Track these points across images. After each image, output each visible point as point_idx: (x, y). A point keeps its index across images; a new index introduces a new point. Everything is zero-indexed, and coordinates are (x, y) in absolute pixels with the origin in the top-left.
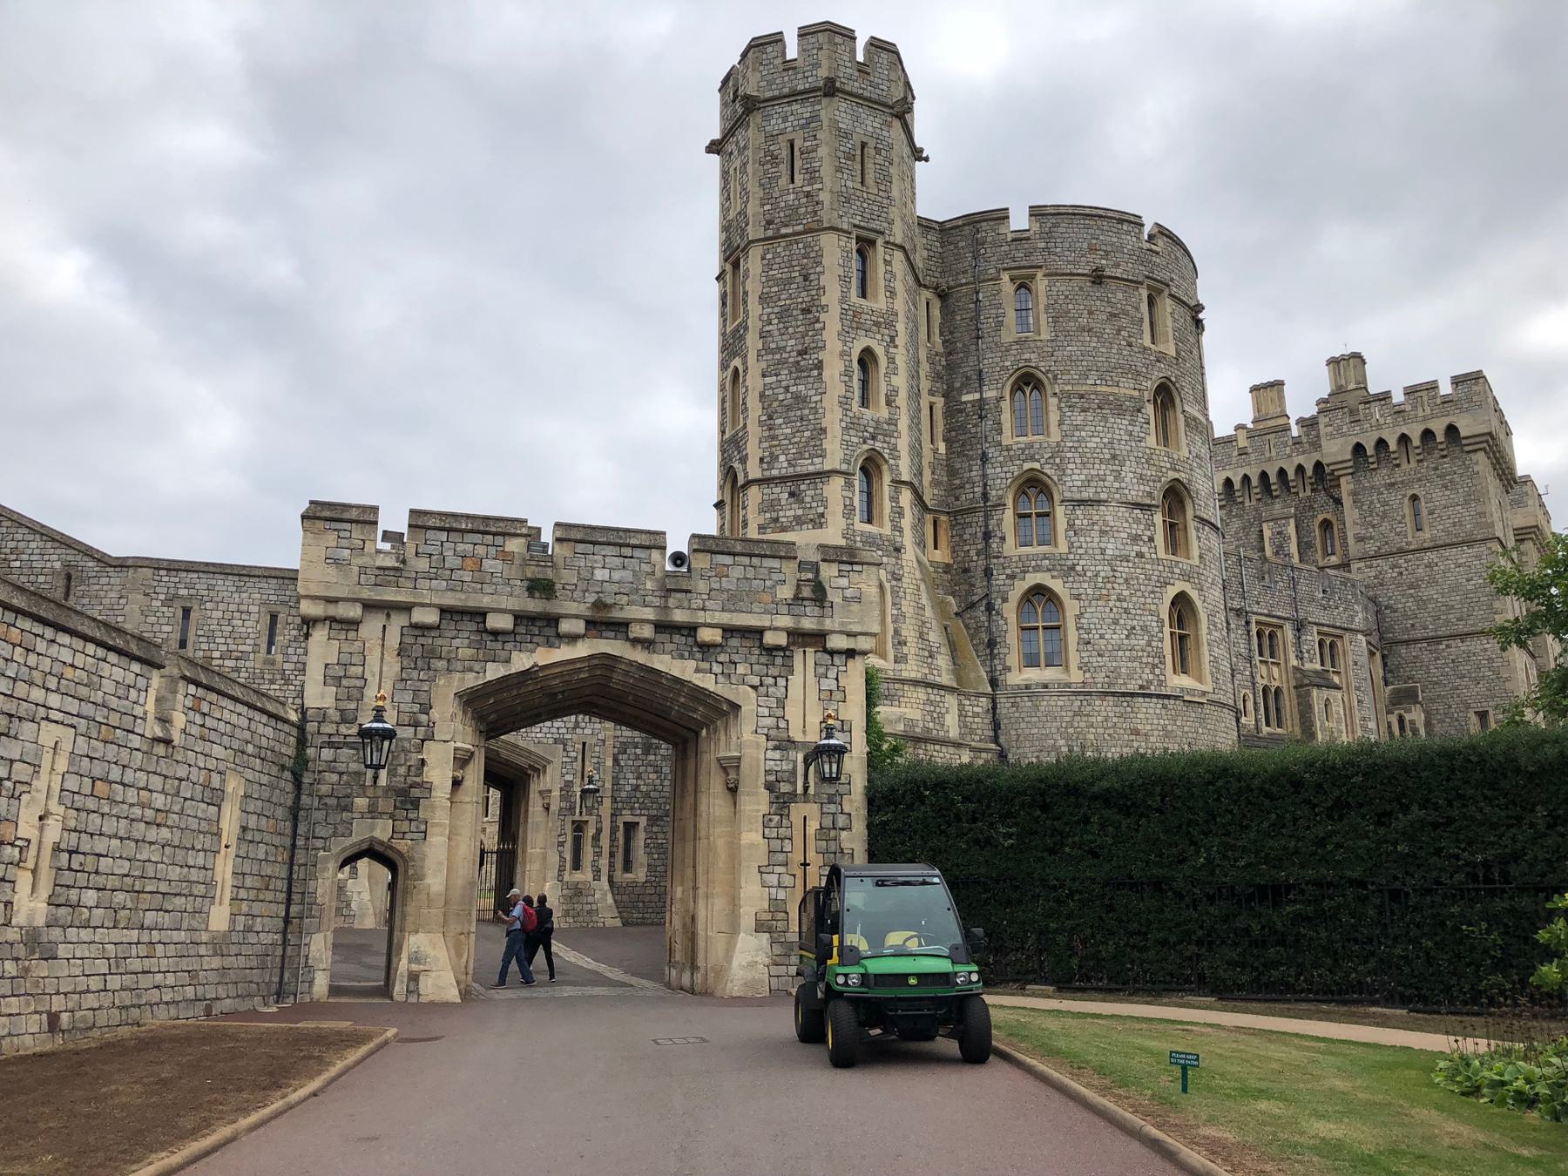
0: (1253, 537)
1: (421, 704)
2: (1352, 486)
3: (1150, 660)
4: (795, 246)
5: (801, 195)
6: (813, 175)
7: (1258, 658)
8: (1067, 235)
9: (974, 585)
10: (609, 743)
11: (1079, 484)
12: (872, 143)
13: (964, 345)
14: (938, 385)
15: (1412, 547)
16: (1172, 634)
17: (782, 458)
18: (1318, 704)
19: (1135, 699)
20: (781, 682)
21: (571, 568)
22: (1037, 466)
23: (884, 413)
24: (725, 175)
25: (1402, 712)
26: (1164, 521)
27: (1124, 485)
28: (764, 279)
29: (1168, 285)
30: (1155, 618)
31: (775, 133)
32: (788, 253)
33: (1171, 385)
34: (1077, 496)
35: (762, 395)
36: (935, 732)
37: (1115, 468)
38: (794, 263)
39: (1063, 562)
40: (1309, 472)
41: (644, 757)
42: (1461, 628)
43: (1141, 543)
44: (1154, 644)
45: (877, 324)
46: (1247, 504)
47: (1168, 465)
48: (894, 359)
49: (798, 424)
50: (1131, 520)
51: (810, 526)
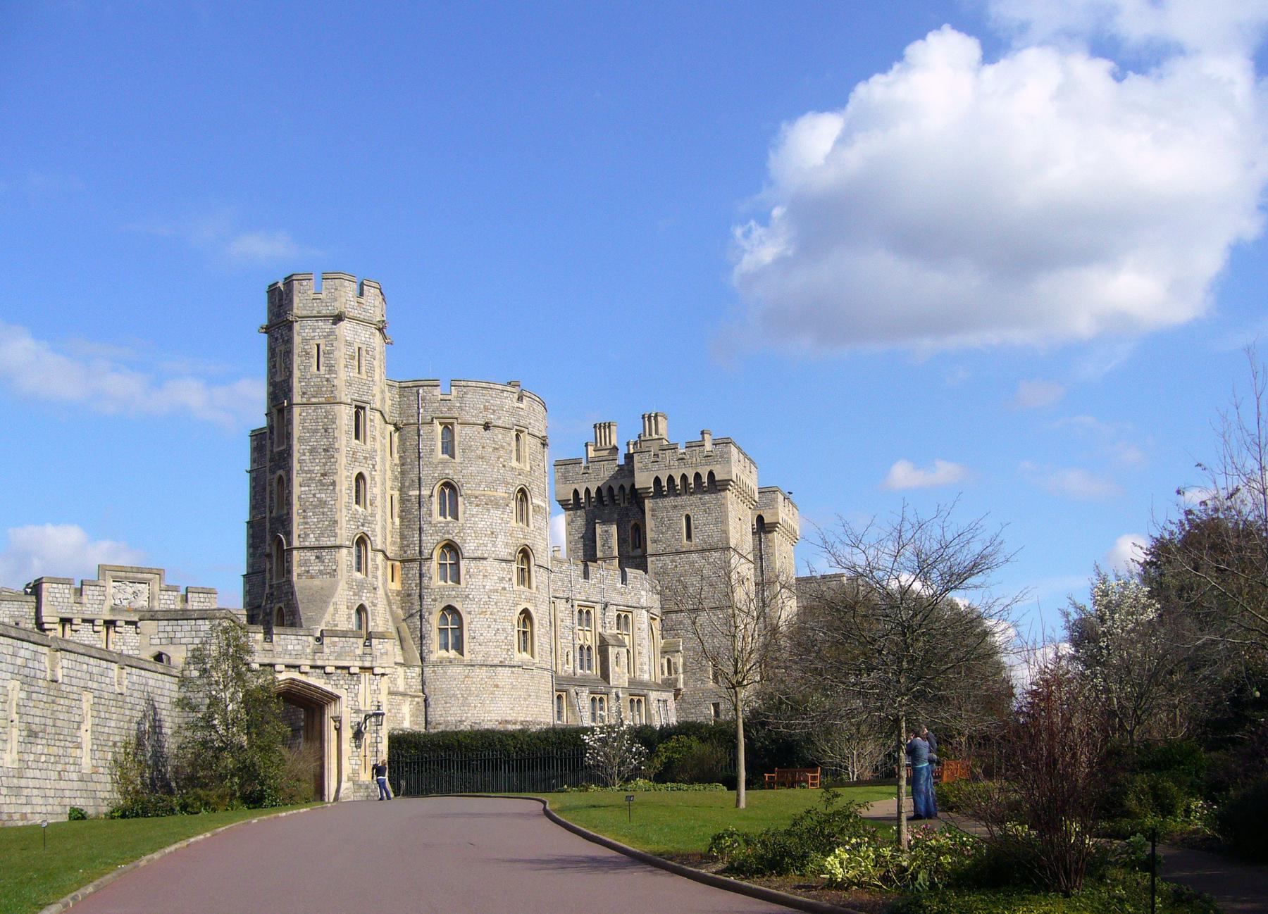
4: (320, 410)
5: (323, 380)
6: (331, 369)
8: (471, 400)
12: (364, 347)
13: (411, 461)
14: (396, 484)
15: (684, 550)
16: (518, 631)
17: (312, 536)
18: (612, 657)
20: (356, 687)
21: (279, 645)
22: (450, 537)
25: (670, 657)
26: (518, 568)
27: (497, 549)
28: (301, 428)
30: (510, 624)
31: (308, 338)
34: (472, 556)
37: (493, 539)
38: (320, 420)
39: (463, 593)
40: (627, 491)
43: (504, 582)
44: (508, 638)
45: (365, 458)
47: (522, 536)
48: (374, 478)
49: (321, 516)
50: (500, 569)
51: (328, 576)
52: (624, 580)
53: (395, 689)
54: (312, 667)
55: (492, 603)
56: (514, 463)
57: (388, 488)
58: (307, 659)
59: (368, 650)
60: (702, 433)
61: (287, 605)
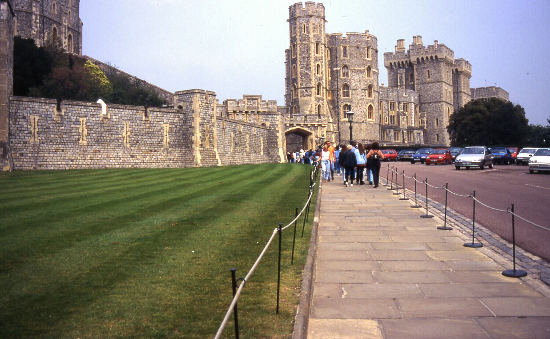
0: (395, 77)
23: (321, 75)
35: (300, 73)
42: (435, 100)
54: (304, 125)
56: (366, 58)
59: (320, 120)
60: (435, 41)
61: (297, 105)
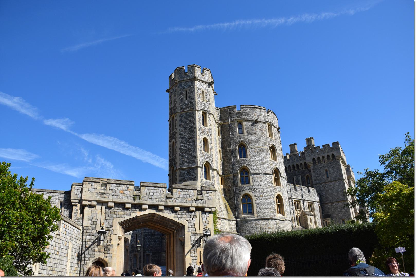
1: (110, 225)
2: (313, 168)
3: (272, 210)
4: (188, 114)
7: (295, 209)
8: (249, 112)
9: (231, 194)
10: (143, 234)
11: (255, 169)
12: (205, 91)
13: (227, 137)
15: (327, 182)
16: (277, 204)
17: (185, 163)
19: (269, 220)
20: (194, 219)
22: (245, 165)
24: (170, 97)
26: (274, 178)
27: (265, 169)
28: (180, 121)
29: (272, 123)
31: (183, 88)
32: (186, 115)
33: (274, 146)
36: (223, 230)
37: (263, 165)
40: (303, 165)
41: (151, 238)
42: (338, 200)
44: (273, 207)
46: (290, 172)
47: (274, 164)
52: (309, 191)
53: (225, 230)
55: (265, 192)
57: (218, 147)
58: (162, 201)
